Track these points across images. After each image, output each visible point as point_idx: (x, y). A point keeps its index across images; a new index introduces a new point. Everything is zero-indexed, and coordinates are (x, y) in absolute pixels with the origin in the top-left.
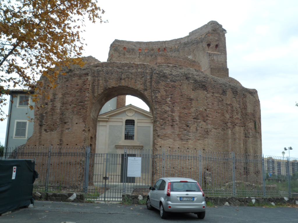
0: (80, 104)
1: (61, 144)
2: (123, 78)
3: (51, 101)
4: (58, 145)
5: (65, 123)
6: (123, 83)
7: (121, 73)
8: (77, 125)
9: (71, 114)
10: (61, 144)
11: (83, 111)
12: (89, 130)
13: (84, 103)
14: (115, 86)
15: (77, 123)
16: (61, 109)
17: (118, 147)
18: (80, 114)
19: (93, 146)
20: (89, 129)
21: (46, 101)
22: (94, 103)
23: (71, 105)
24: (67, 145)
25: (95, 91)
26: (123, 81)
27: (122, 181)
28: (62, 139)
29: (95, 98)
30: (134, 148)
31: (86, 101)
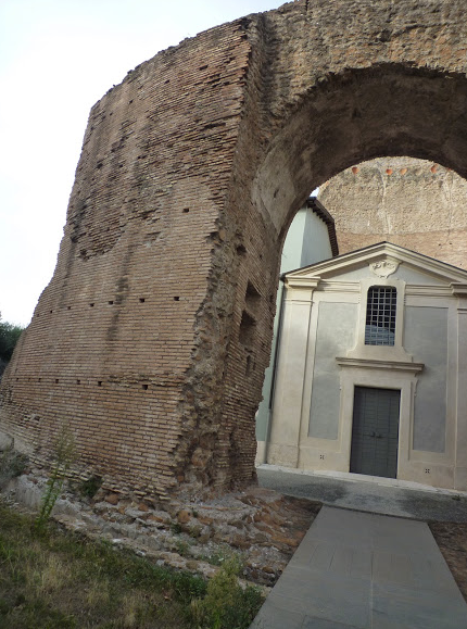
0: (206, 133)
1: (120, 300)
2: (395, 31)
3: (113, 151)
4: (111, 303)
5: (145, 215)
6: (395, 53)
7: (387, 14)
8: (187, 215)
9: (170, 176)
10: (120, 300)
11: (216, 159)
12: (241, 250)
13: (224, 124)
14: (361, 66)
15: (186, 210)
16: (137, 165)
17: (343, 363)
18: (202, 170)
19: (260, 329)
20: (238, 242)
21: (99, 156)
22: (267, 141)
23: (170, 146)
24: (142, 300)
25: (275, 94)
26: (395, 44)
27: (352, 470)
28: (126, 280)
29: (273, 122)
30: (392, 370)
31: (231, 117)
